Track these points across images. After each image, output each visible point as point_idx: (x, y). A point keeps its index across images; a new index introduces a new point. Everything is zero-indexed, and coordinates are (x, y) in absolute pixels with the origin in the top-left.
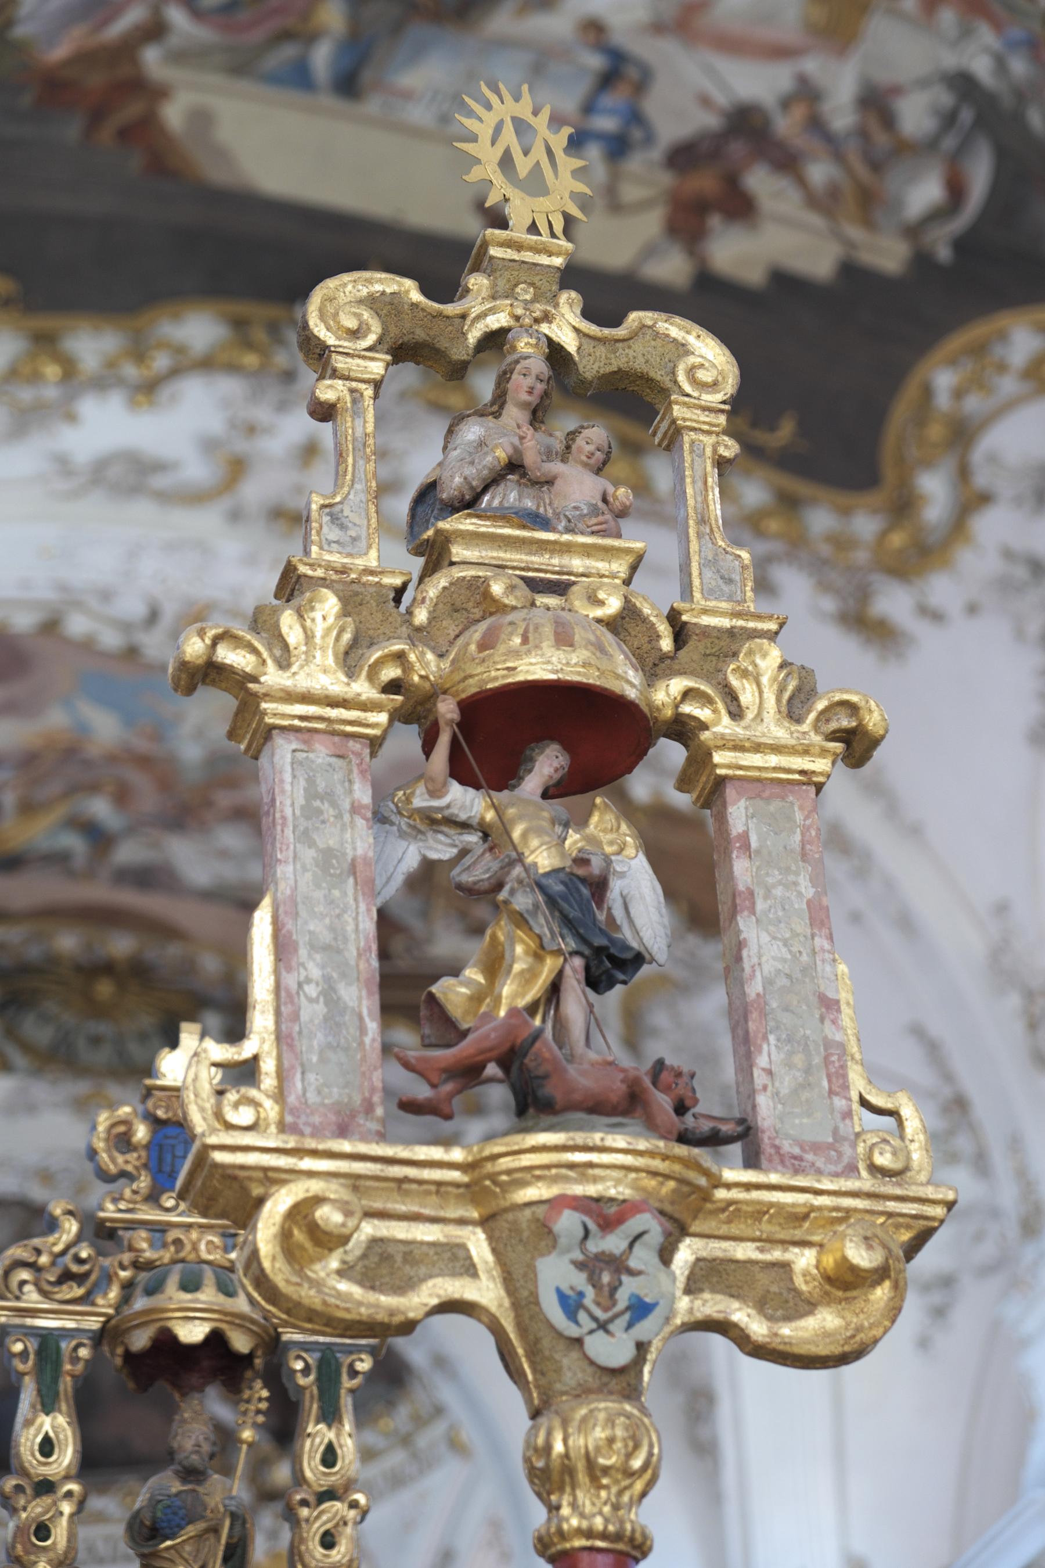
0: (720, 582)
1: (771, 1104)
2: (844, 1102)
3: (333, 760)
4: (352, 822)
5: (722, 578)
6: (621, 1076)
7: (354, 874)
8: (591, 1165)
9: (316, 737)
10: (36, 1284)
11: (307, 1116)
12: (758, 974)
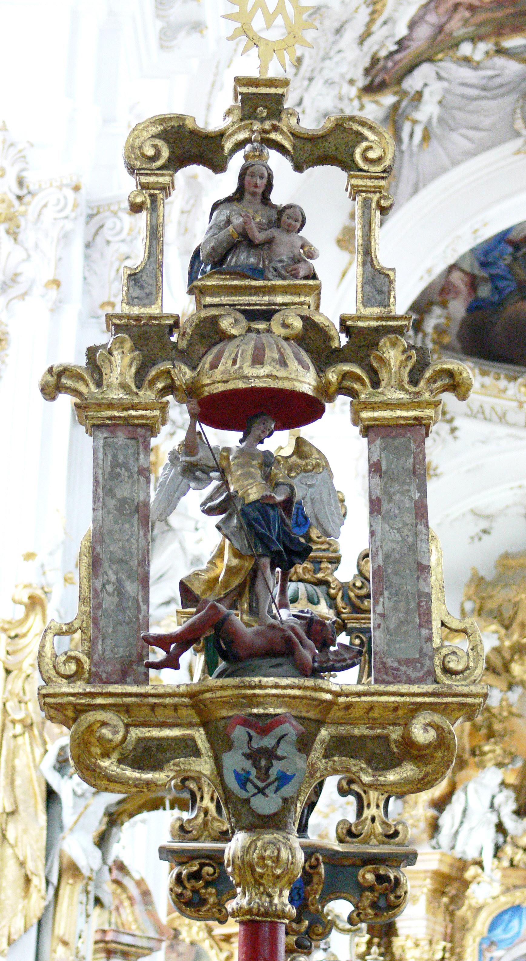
0: (375, 293)
1: (383, 637)
2: (427, 631)
3: (128, 441)
4: (138, 479)
5: (377, 290)
6: (281, 634)
7: (138, 512)
8: (255, 695)
9: (120, 428)
11: (104, 666)
12: (380, 553)
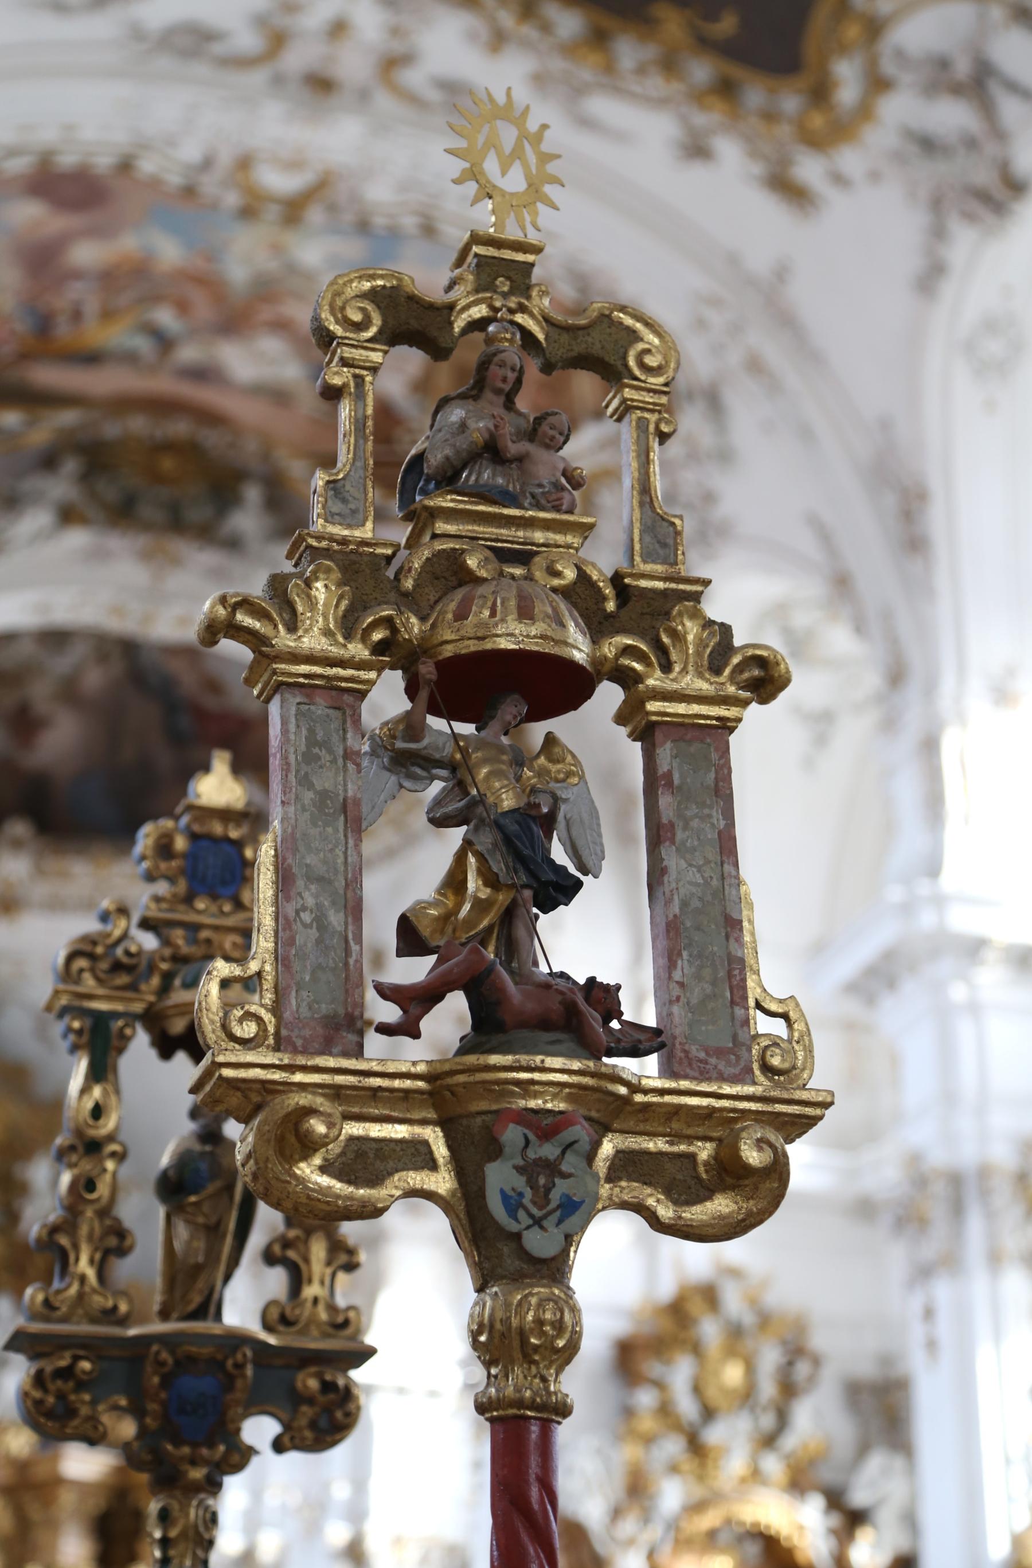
0: (657, 546)
1: (683, 1014)
2: (743, 1011)
3: (331, 711)
4: (345, 766)
5: (659, 542)
6: (560, 998)
7: (345, 812)
8: (532, 1082)
9: (318, 691)
10: (92, 970)
11: (300, 1029)
12: (676, 897)
